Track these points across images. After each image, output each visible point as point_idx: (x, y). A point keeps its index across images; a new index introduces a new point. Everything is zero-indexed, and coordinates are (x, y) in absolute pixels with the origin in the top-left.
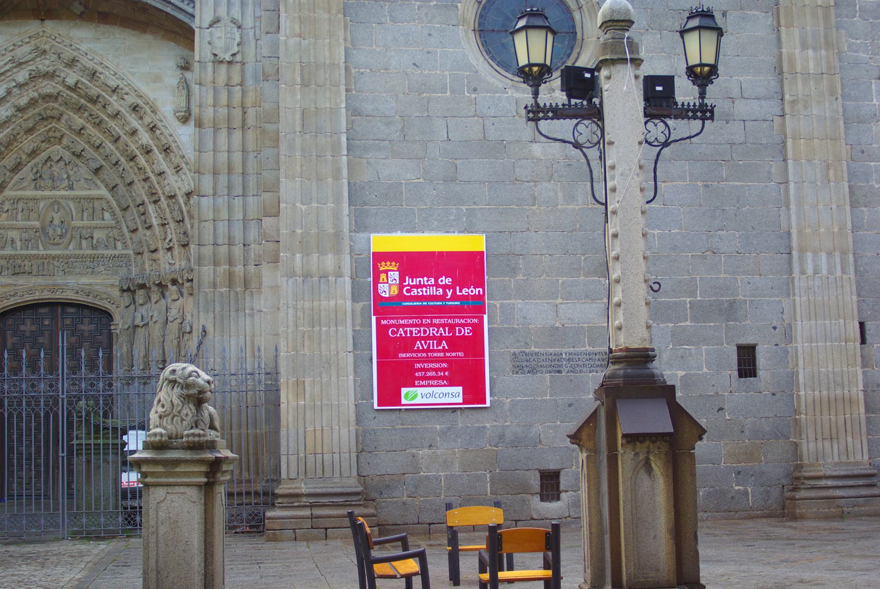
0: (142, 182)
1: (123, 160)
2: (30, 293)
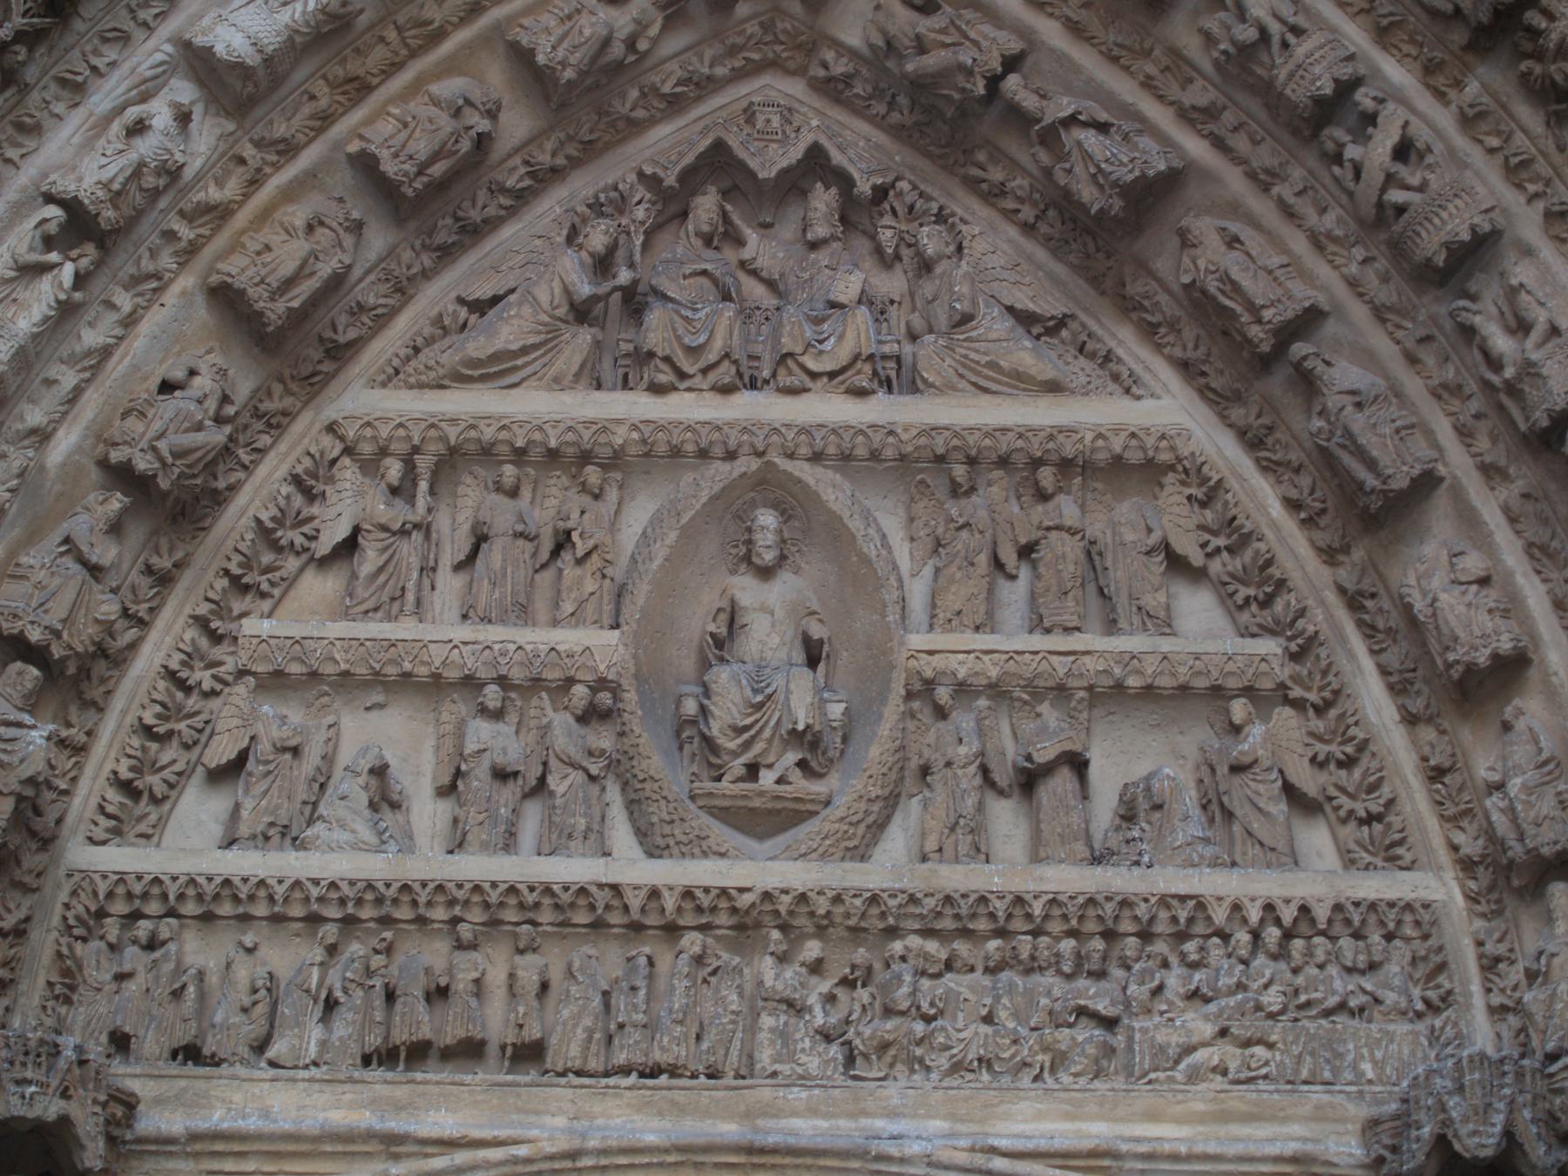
1: (1396, 72)
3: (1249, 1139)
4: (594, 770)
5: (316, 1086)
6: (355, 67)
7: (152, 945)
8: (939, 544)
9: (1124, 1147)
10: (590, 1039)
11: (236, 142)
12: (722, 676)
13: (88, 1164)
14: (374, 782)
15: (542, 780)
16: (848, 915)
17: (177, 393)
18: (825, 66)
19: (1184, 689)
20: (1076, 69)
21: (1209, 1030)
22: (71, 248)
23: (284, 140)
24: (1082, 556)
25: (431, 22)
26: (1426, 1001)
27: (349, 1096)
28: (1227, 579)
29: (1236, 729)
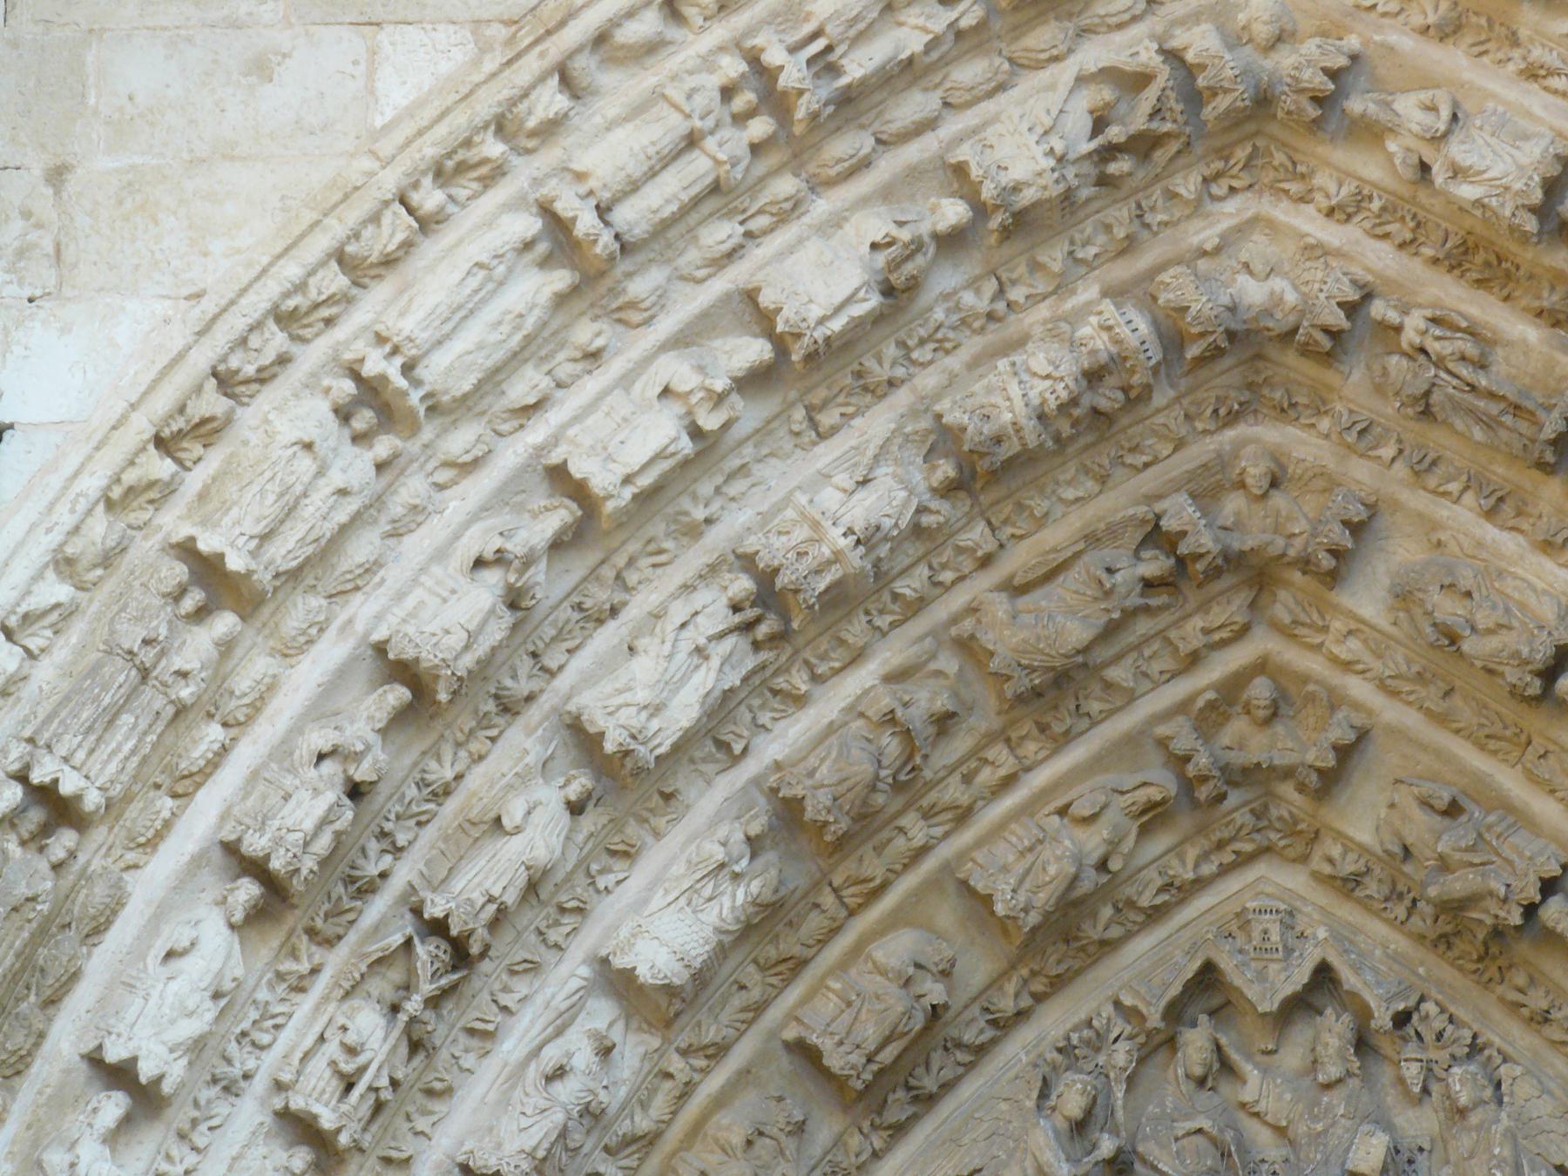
6: (790, 945)
18: (1330, 861)
25: (871, 880)
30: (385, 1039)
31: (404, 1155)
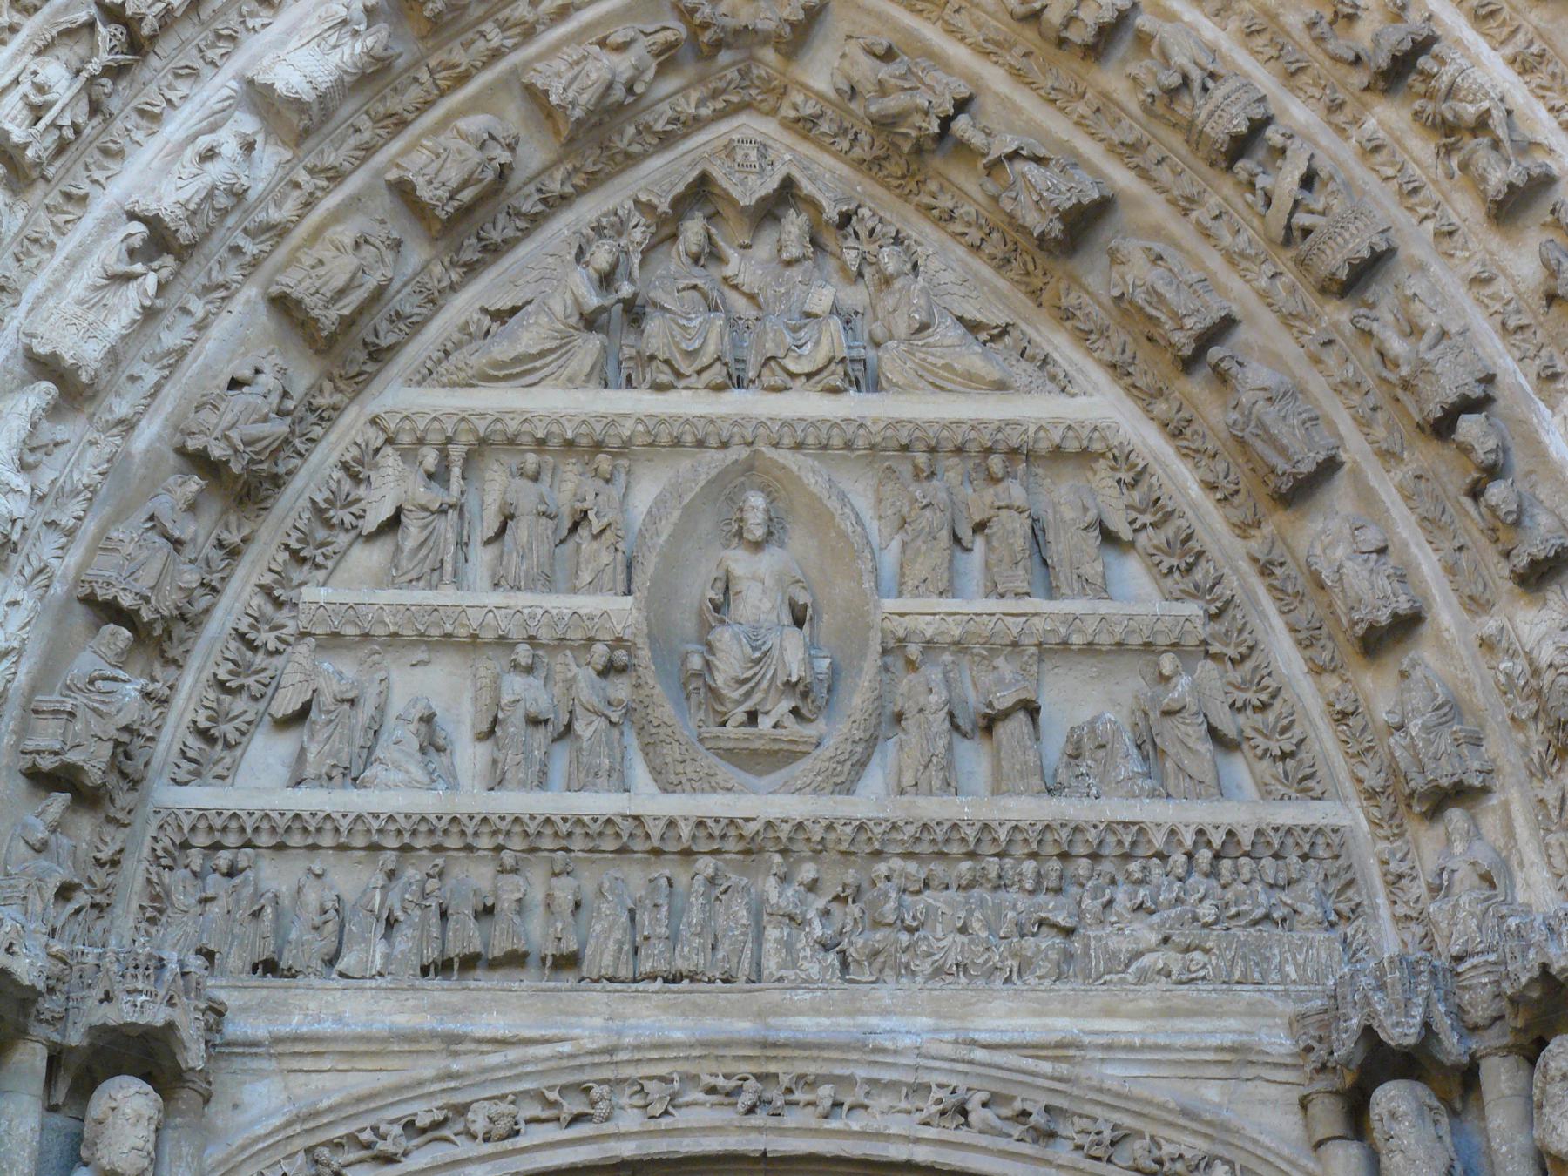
0: (1482, 242)
2: (573, 1106)
3: (1192, 1032)
4: (615, 718)
5: (383, 994)
6: (394, 104)
7: (231, 873)
8: (904, 523)
9: (1086, 1040)
10: (620, 950)
11: (292, 169)
12: (723, 637)
13: (191, 1065)
14: (423, 728)
15: (569, 727)
16: (839, 841)
17: (245, 389)
18: (795, 107)
19: (1119, 644)
20: (1018, 110)
21: (1154, 938)
22: (151, 260)
23: (334, 167)
24: (1029, 532)
25: (458, 66)
26: (1338, 913)
27: (411, 1003)
28: (1152, 551)
29: (1167, 679)
30: (70, 87)
31: (81, 192)
